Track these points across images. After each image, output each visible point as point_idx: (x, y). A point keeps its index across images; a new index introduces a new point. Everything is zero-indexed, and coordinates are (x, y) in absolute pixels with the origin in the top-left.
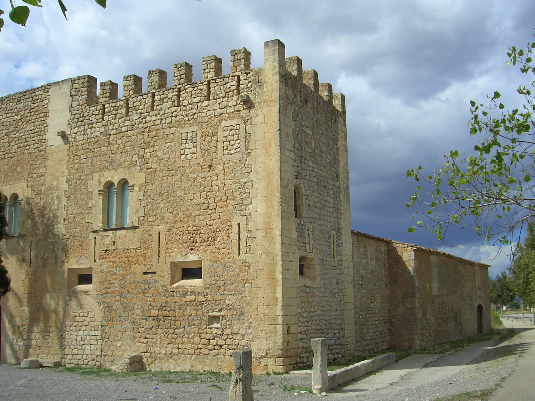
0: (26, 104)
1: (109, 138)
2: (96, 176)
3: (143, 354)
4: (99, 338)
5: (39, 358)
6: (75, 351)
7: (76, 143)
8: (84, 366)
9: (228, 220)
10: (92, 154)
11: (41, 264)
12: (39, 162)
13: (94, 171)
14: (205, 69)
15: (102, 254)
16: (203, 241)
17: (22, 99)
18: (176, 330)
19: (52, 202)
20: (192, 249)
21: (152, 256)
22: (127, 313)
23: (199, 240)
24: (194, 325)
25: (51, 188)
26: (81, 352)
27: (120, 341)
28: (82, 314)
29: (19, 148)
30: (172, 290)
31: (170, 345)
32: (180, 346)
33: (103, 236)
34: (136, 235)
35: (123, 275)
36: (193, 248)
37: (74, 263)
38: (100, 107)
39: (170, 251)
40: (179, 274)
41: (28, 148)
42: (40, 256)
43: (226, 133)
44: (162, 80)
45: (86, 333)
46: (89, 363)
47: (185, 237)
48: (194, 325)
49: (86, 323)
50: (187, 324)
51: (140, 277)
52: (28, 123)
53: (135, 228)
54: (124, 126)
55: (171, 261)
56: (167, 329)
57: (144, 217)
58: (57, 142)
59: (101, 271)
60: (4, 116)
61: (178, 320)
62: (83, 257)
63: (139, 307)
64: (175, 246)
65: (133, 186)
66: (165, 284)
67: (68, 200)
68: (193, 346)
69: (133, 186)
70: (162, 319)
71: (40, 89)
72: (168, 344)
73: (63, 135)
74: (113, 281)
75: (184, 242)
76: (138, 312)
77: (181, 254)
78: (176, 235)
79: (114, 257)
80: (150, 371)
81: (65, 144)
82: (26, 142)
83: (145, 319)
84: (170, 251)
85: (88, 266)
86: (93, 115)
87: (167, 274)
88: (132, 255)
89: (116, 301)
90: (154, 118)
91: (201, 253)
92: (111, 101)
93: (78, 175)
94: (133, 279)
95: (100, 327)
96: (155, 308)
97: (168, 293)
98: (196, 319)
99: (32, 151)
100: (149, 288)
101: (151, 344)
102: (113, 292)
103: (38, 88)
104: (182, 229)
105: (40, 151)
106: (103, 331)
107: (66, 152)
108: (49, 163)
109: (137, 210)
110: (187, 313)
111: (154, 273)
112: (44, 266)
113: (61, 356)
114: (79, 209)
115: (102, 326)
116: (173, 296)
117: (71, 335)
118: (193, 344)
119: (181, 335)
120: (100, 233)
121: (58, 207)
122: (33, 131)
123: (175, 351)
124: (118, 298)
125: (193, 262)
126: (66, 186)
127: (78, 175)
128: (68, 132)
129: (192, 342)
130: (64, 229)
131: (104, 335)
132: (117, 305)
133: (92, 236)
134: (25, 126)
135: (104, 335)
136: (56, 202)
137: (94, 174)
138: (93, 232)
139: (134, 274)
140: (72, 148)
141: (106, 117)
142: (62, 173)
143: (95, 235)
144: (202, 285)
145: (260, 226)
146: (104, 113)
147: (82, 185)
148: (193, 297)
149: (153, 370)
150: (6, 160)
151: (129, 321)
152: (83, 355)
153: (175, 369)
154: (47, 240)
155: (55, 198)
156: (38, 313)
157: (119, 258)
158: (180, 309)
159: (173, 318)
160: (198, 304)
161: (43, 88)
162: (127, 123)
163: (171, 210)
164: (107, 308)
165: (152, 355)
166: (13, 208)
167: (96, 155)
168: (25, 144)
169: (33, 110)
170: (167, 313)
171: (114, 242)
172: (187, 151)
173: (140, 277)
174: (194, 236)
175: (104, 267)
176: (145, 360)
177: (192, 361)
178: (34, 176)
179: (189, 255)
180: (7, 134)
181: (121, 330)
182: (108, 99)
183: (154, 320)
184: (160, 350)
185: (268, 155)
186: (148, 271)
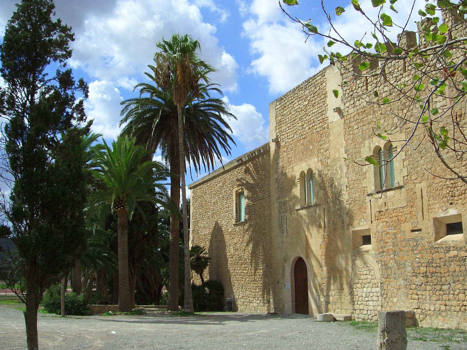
0: (311, 90)
1: (373, 106)
2: (367, 142)
3: (415, 310)
4: (379, 294)
5: (336, 312)
6: (361, 307)
7: (349, 116)
8: (369, 321)
10: (362, 124)
11: (332, 228)
12: (324, 138)
13: (364, 139)
14: (445, 20)
15: (376, 215)
16: (460, 194)
17: (307, 86)
18: (443, 287)
19: (336, 172)
20: (451, 204)
21: (418, 213)
22: (400, 271)
23: (457, 193)
24: (458, 281)
25: (334, 160)
26: (366, 308)
27: (395, 297)
28: (365, 272)
29: (309, 129)
30: (437, 246)
31: (438, 301)
32: (447, 303)
33: (376, 198)
34: (402, 194)
35: (395, 234)
36: (453, 202)
37: (361, 225)
38: (363, 79)
39: (432, 207)
40: (444, 229)
41: (315, 127)
42: (331, 222)
44: (411, 41)
45: (369, 290)
46: (373, 318)
47: (444, 192)
48: (458, 281)
49: (369, 281)
50: (452, 281)
51: (409, 235)
52: (313, 106)
53: (401, 187)
54: (384, 92)
55: (434, 217)
56: (435, 285)
57: (407, 176)
58: (333, 117)
59: (377, 231)
60: (297, 104)
61: (444, 276)
62: (362, 220)
63: (410, 264)
64: (436, 201)
65: (396, 147)
66: (430, 240)
67: (348, 169)
68: (458, 302)
69: (396, 147)
70: (430, 276)
71: (319, 74)
72: (436, 301)
73: (338, 110)
74: (387, 240)
75: (443, 197)
76: (409, 269)
77: (442, 209)
78: (436, 191)
79: (386, 218)
80: (422, 327)
81: (341, 119)
82: (314, 122)
83: (416, 276)
84: (432, 207)
85: (367, 228)
86: (359, 87)
87: (431, 230)
88: (401, 214)
89: (391, 259)
90: (407, 79)
91: (460, 207)
92: (371, 72)
93: (353, 144)
94: (403, 237)
95: (379, 284)
96: (423, 265)
97: (434, 250)
98: (459, 275)
99: (318, 130)
100: (417, 245)
101: (422, 301)
103: (318, 74)
104: (441, 183)
105: (324, 129)
106: (382, 288)
107: (342, 125)
108: (331, 138)
109: (402, 170)
110: (451, 269)
111: (420, 230)
112: (335, 230)
113: (351, 311)
114: (357, 176)
115: (381, 283)
116: (438, 252)
117: (358, 291)
118: (458, 300)
119: (447, 292)
120: (374, 196)
121: (341, 176)
122: (318, 112)
123: (443, 308)
125: (453, 216)
127: (353, 144)
128: (342, 108)
129: (457, 299)
130: (347, 195)
131: (383, 291)
132: (392, 263)
133: (368, 199)
134: (312, 109)
135: (383, 291)
137: (365, 142)
138: (368, 195)
139: (404, 232)
140: (346, 121)
141: (369, 87)
142: (342, 145)
143: (370, 198)
144: (463, 239)
146: (367, 84)
147: (356, 153)
148: (455, 253)
149: (424, 326)
150: (302, 141)
151: (402, 278)
152: (367, 311)
153: (443, 326)
154: (336, 207)
155: (338, 168)
156: (334, 272)
157: (390, 218)
158: (445, 265)
159: (439, 275)
160: (461, 259)
161: (321, 73)
162: (386, 89)
163: (429, 166)
164: (384, 266)
165: (423, 311)
166: (311, 182)
167: (365, 124)
168: (314, 124)
169: (316, 94)
170: (434, 269)
171: (385, 203)
173: (409, 235)
174: (452, 189)
175: (379, 227)
176: (417, 316)
178: (322, 151)
179: (449, 209)
180: (301, 119)
181: (396, 287)
182: (369, 70)
183: (423, 277)
184: (429, 307)
186: (415, 229)
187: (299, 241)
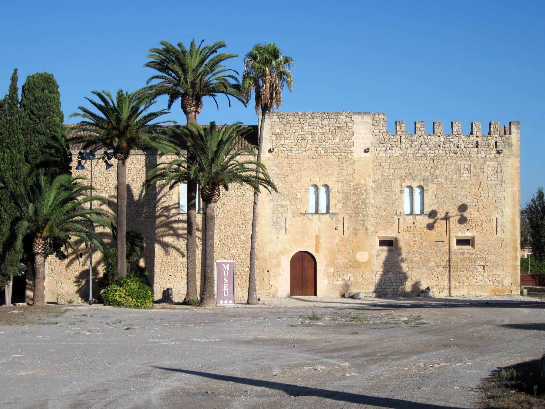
9: (491, 216)
20: (468, 230)
43: (489, 169)
76: (433, 264)
89: (416, 256)
102: (414, 251)
121: (366, 197)
124: (416, 255)
126: (373, 185)
136: (365, 194)
143: (399, 217)
145: (509, 220)
172: (464, 175)
177: (468, 290)
185: (513, 184)
187: (306, 239)
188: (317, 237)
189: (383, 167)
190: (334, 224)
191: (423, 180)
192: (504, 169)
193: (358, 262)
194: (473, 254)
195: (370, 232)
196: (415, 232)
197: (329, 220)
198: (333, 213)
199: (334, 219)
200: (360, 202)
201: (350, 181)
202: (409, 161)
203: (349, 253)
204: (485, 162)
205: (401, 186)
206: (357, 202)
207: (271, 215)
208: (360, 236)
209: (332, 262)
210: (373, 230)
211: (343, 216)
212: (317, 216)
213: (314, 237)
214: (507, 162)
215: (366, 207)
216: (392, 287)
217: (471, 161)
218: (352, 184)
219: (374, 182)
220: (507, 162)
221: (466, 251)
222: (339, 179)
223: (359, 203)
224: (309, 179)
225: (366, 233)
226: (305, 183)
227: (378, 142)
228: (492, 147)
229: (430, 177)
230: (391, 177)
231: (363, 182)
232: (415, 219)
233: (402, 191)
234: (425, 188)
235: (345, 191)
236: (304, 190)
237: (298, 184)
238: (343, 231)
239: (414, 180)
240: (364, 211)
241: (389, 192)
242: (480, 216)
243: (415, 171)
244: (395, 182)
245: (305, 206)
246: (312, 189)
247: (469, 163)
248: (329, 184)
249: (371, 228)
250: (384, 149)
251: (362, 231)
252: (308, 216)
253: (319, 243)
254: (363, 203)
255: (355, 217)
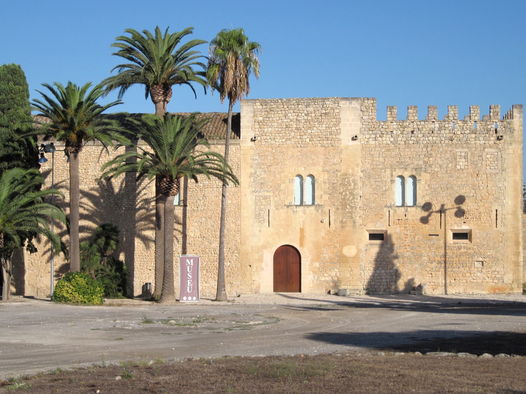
9: (490, 207)
76: (426, 258)
89: (407, 251)
102: (405, 245)
124: (408, 249)
136: (353, 184)
143: (390, 209)
172: (461, 163)
177: (464, 287)
187: (290, 232)
188: (302, 230)
189: (372, 155)
190: (320, 217)
191: (416, 169)
192: (504, 156)
193: (345, 257)
194: (470, 248)
195: (358, 224)
196: (407, 225)
197: (315, 212)
198: (319, 205)
199: (320, 211)
200: (348, 193)
201: (337, 170)
202: (400, 149)
203: (336, 247)
204: (484, 150)
205: (392, 175)
206: (344, 193)
207: (253, 207)
208: (347, 229)
209: (318, 257)
210: (361, 223)
211: (329, 208)
212: (302, 208)
213: (299, 230)
214: (508, 149)
215: (354, 198)
216: (382, 284)
217: (468, 148)
218: (339, 174)
219: (362, 171)
220: (508, 149)
221: (463, 245)
222: (324, 169)
223: (346, 194)
224: (293, 169)
225: (354, 226)
226: (289, 173)
227: (367, 129)
228: (491, 133)
229: (423, 166)
230: (381, 167)
231: (350, 172)
232: (407, 211)
233: (392, 181)
234: (418, 178)
235: (332, 181)
236: (287, 181)
237: (282, 174)
238: (330, 224)
239: (406, 169)
240: (351, 203)
241: (378, 182)
242: (478, 208)
243: (407, 160)
244: (385, 172)
245: (289, 198)
246: (298, 180)
247: (467, 150)
248: (314, 174)
249: (359, 221)
250: (374, 136)
251: (350, 224)
252: (292, 207)
253: (304, 236)
254: (351, 194)
255: (342, 209)
